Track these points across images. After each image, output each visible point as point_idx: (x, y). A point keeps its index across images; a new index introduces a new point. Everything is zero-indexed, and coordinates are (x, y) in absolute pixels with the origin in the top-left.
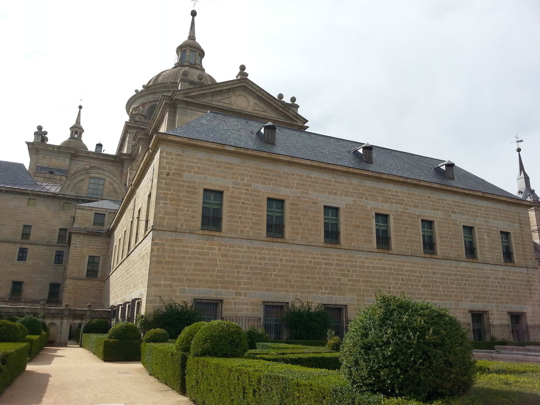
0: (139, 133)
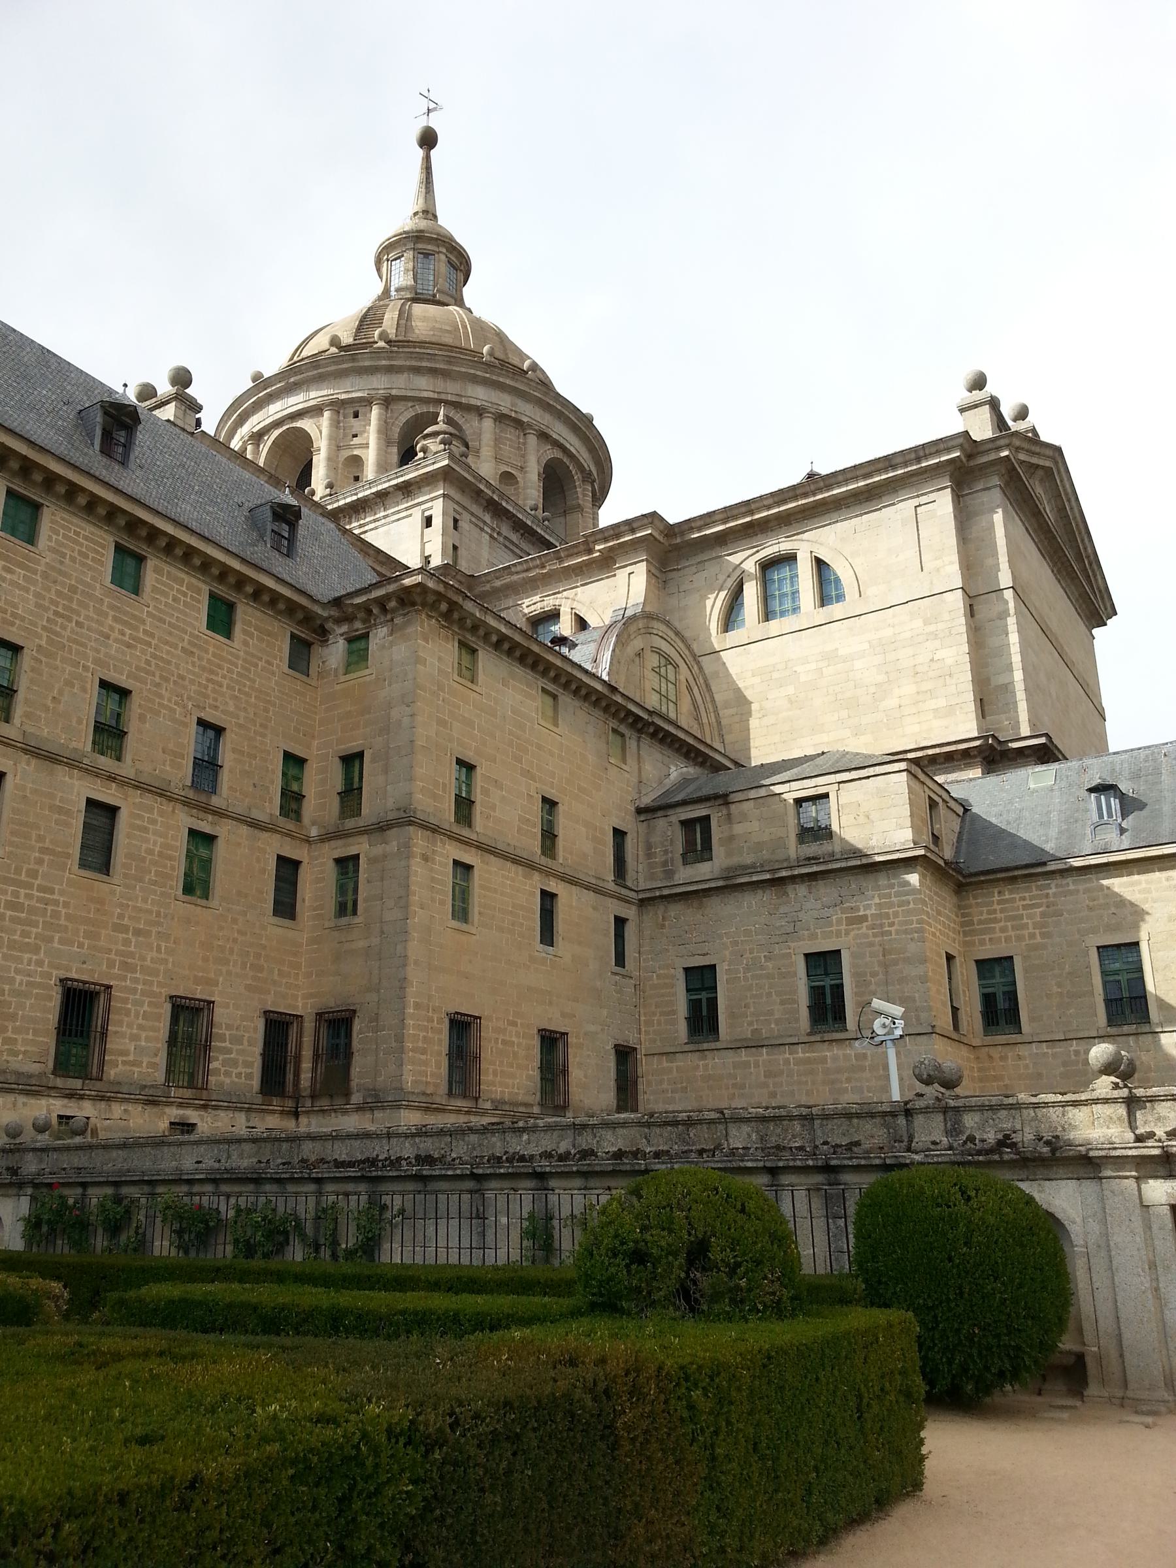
0: (656, 522)
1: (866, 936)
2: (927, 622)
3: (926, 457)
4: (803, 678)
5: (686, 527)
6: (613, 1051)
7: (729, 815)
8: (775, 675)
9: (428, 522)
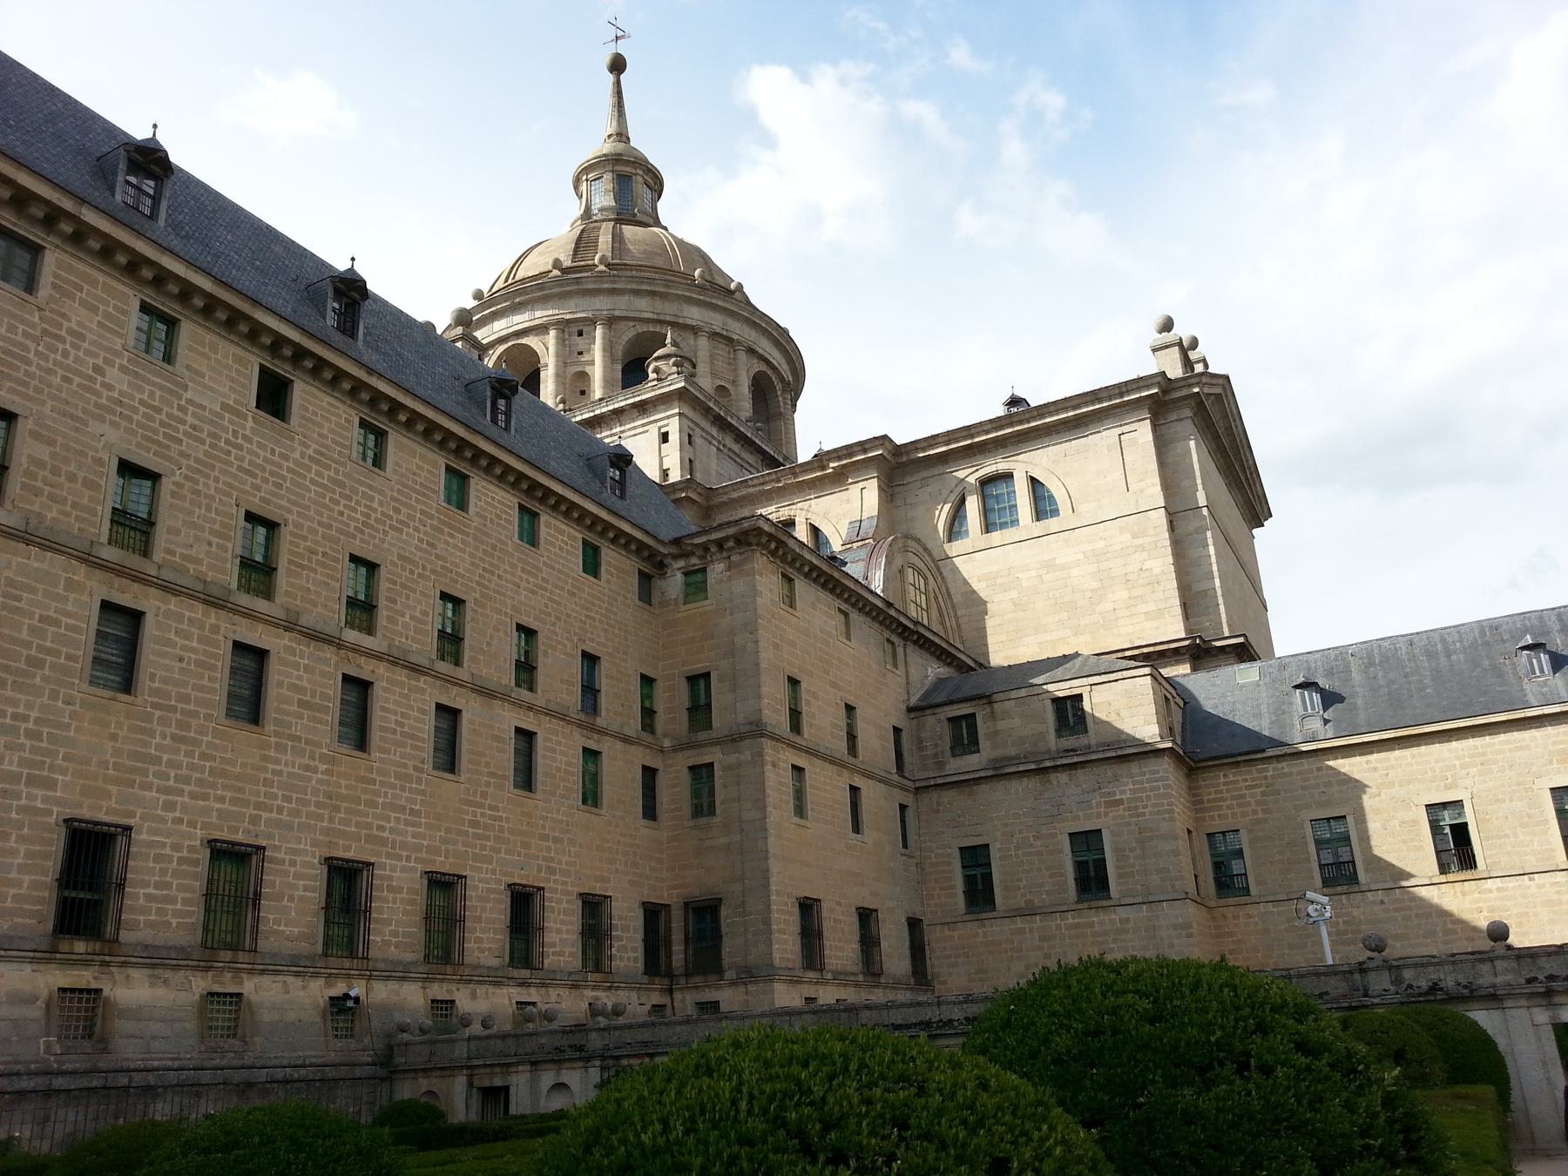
0: (886, 443)
1: (1123, 817)
2: (1135, 536)
3: (1128, 392)
4: (1025, 584)
5: (912, 447)
6: (906, 924)
7: (992, 713)
8: (999, 581)
9: (665, 438)
